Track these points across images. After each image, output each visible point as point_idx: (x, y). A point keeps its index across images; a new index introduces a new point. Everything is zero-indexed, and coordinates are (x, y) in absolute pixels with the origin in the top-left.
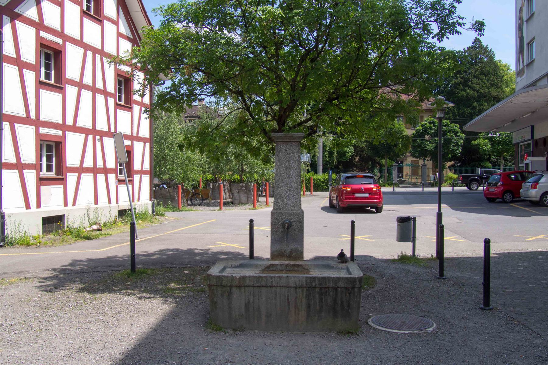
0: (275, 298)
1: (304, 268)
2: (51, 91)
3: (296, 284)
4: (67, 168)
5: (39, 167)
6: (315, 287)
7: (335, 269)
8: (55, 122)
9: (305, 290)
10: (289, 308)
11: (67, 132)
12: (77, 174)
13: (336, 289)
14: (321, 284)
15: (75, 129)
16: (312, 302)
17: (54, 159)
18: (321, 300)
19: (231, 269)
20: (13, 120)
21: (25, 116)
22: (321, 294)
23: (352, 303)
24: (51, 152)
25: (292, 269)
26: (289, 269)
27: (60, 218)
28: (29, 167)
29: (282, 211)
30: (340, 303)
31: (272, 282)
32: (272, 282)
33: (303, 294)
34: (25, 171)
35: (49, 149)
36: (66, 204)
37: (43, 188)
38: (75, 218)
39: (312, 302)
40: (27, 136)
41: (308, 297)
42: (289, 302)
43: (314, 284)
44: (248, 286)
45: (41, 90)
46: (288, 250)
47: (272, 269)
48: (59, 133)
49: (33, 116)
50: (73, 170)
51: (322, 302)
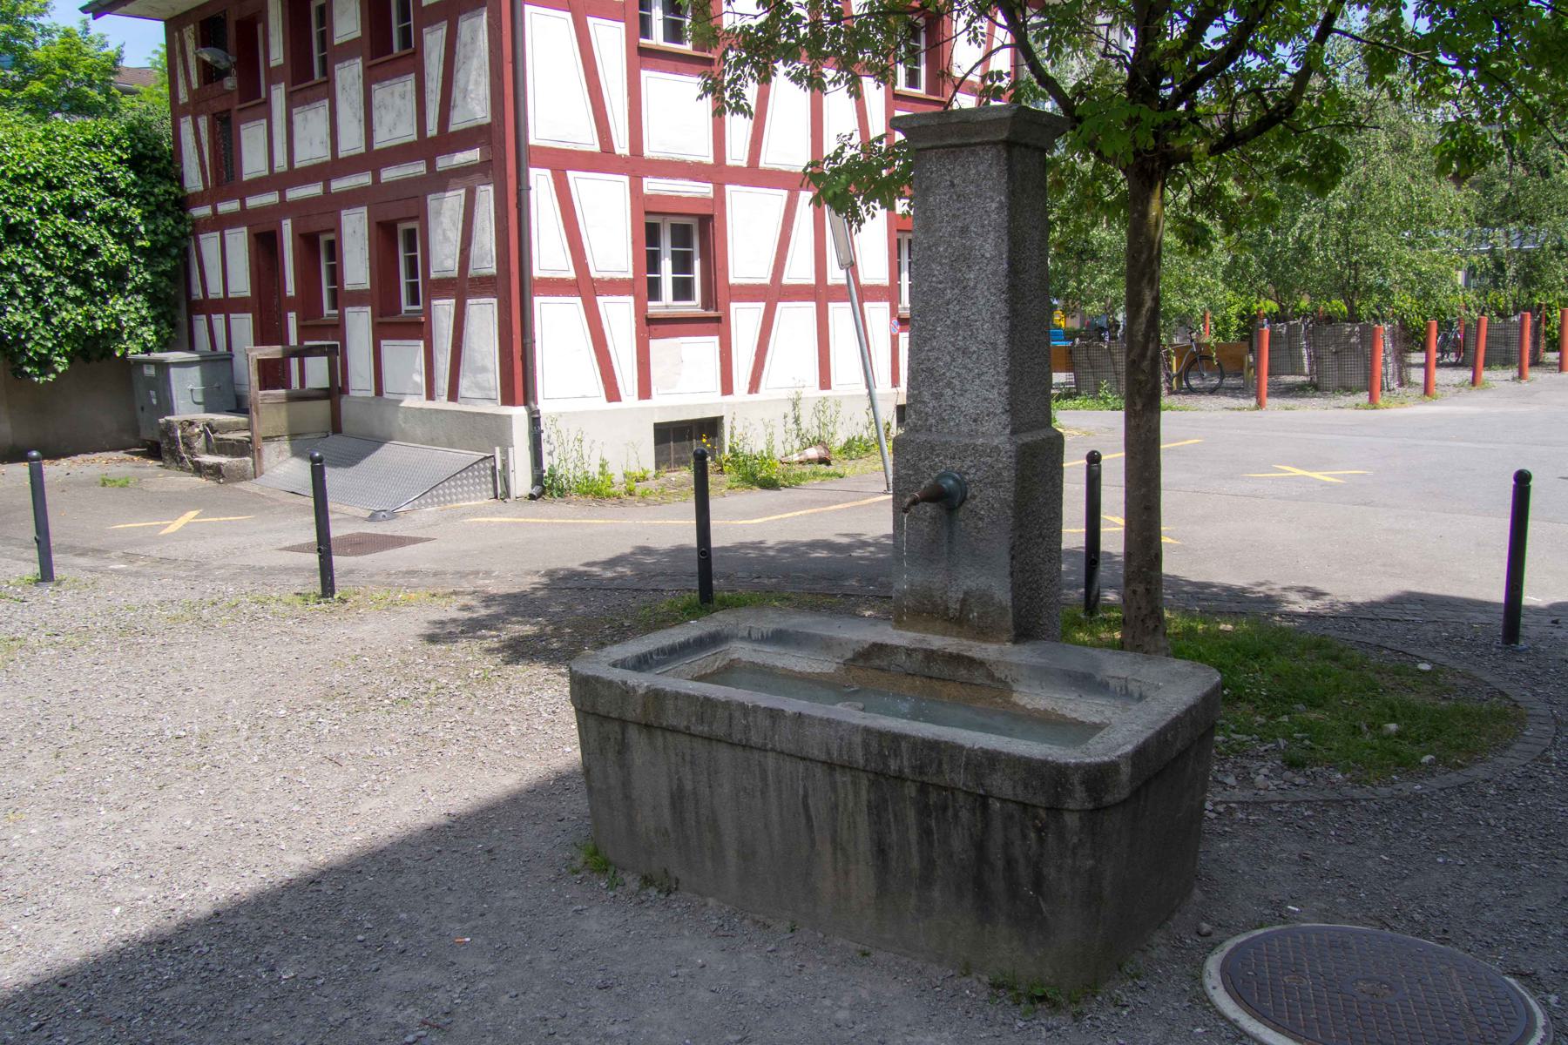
0: (762, 793)
1: (991, 676)
2: (677, 72)
3: (828, 753)
4: (730, 287)
5: (643, 288)
6: (900, 778)
7: (1114, 695)
8: (690, 159)
9: (864, 783)
10: (813, 843)
11: (728, 188)
12: (762, 305)
13: (983, 801)
14: (920, 769)
15: (754, 175)
16: (894, 837)
17: (697, 264)
18: (926, 833)
19: (748, 646)
20: (562, 162)
21: (597, 148)
22: (924, 811)
23: (1051, 873)
24: (688, 243)
25: (946, 672)
26: (935, 670)
27: (711, 427)
28: (614, 287)
29: (934, 437)
30: (1000, 864)
31: (747, 727)
32: (747, 727)
33: (857, 794)
34: (600, 300)
35: (682, 235)
36: (727, 388)
37: (656, 346)
38: (754, 426)
39: (894, 837)
40: (606, 207)
41: (877, 811)
42: (809, 818)
43: (893, 765)
44: (674, 730)
45: (644, 74)
46: (955, 595)
47: (877, 662)
48: (705, 189)
49: (622, 147)
50: (749, 293)
51: (931, 844)
